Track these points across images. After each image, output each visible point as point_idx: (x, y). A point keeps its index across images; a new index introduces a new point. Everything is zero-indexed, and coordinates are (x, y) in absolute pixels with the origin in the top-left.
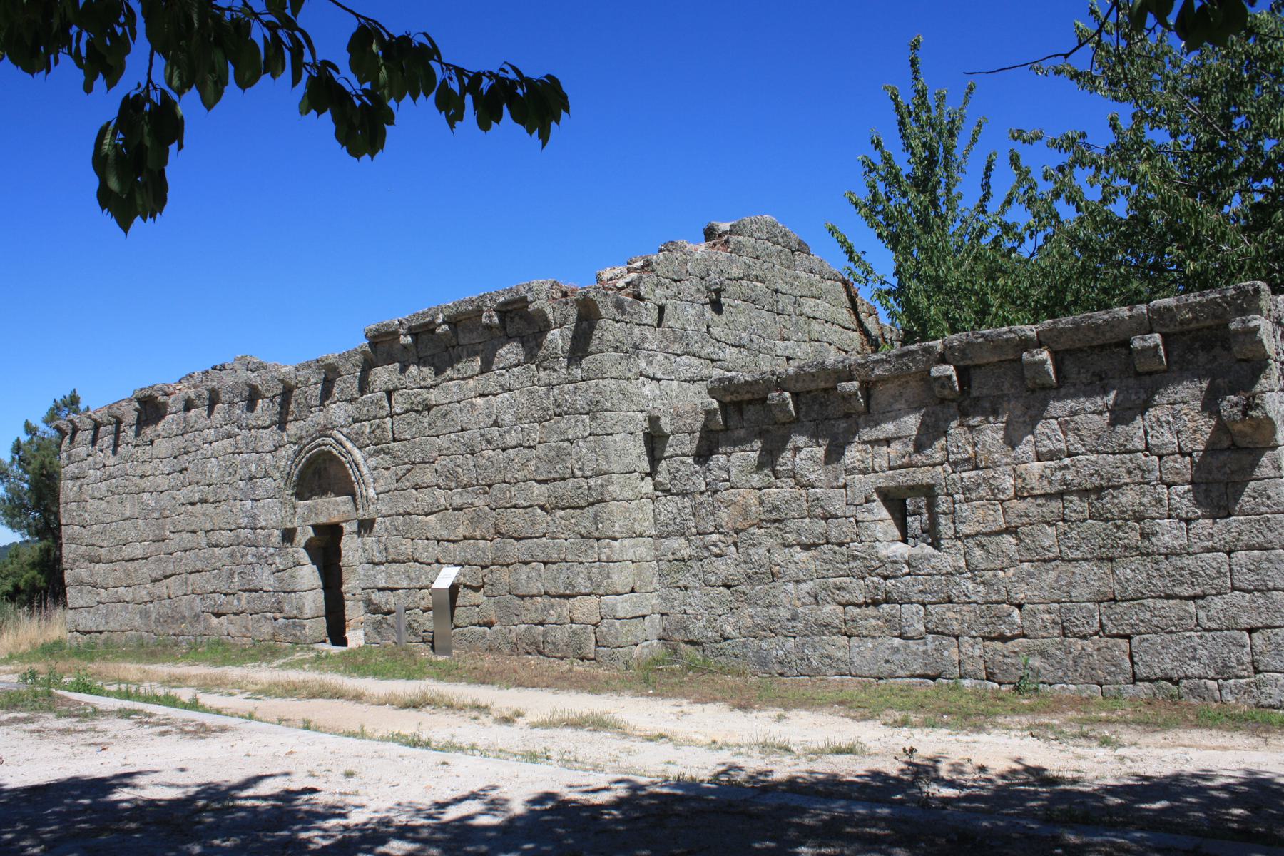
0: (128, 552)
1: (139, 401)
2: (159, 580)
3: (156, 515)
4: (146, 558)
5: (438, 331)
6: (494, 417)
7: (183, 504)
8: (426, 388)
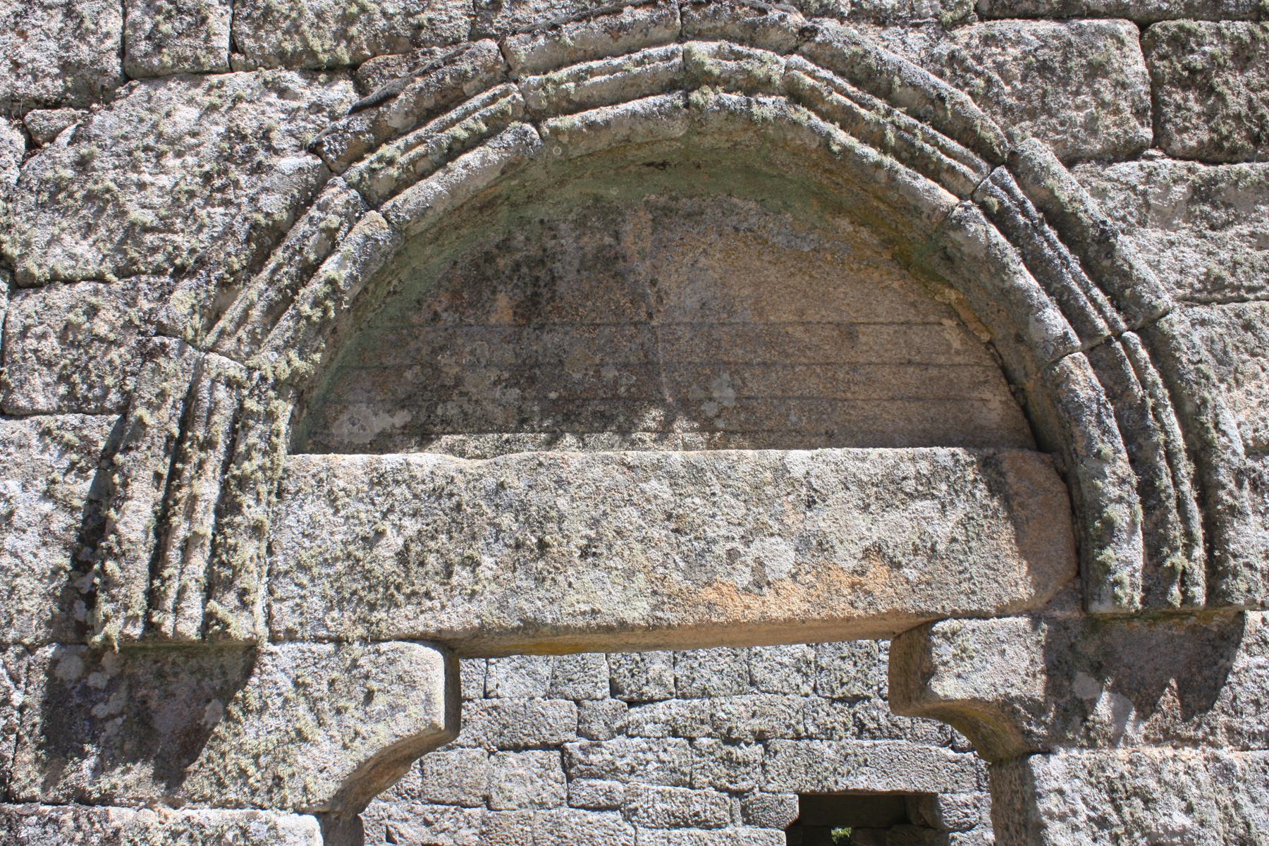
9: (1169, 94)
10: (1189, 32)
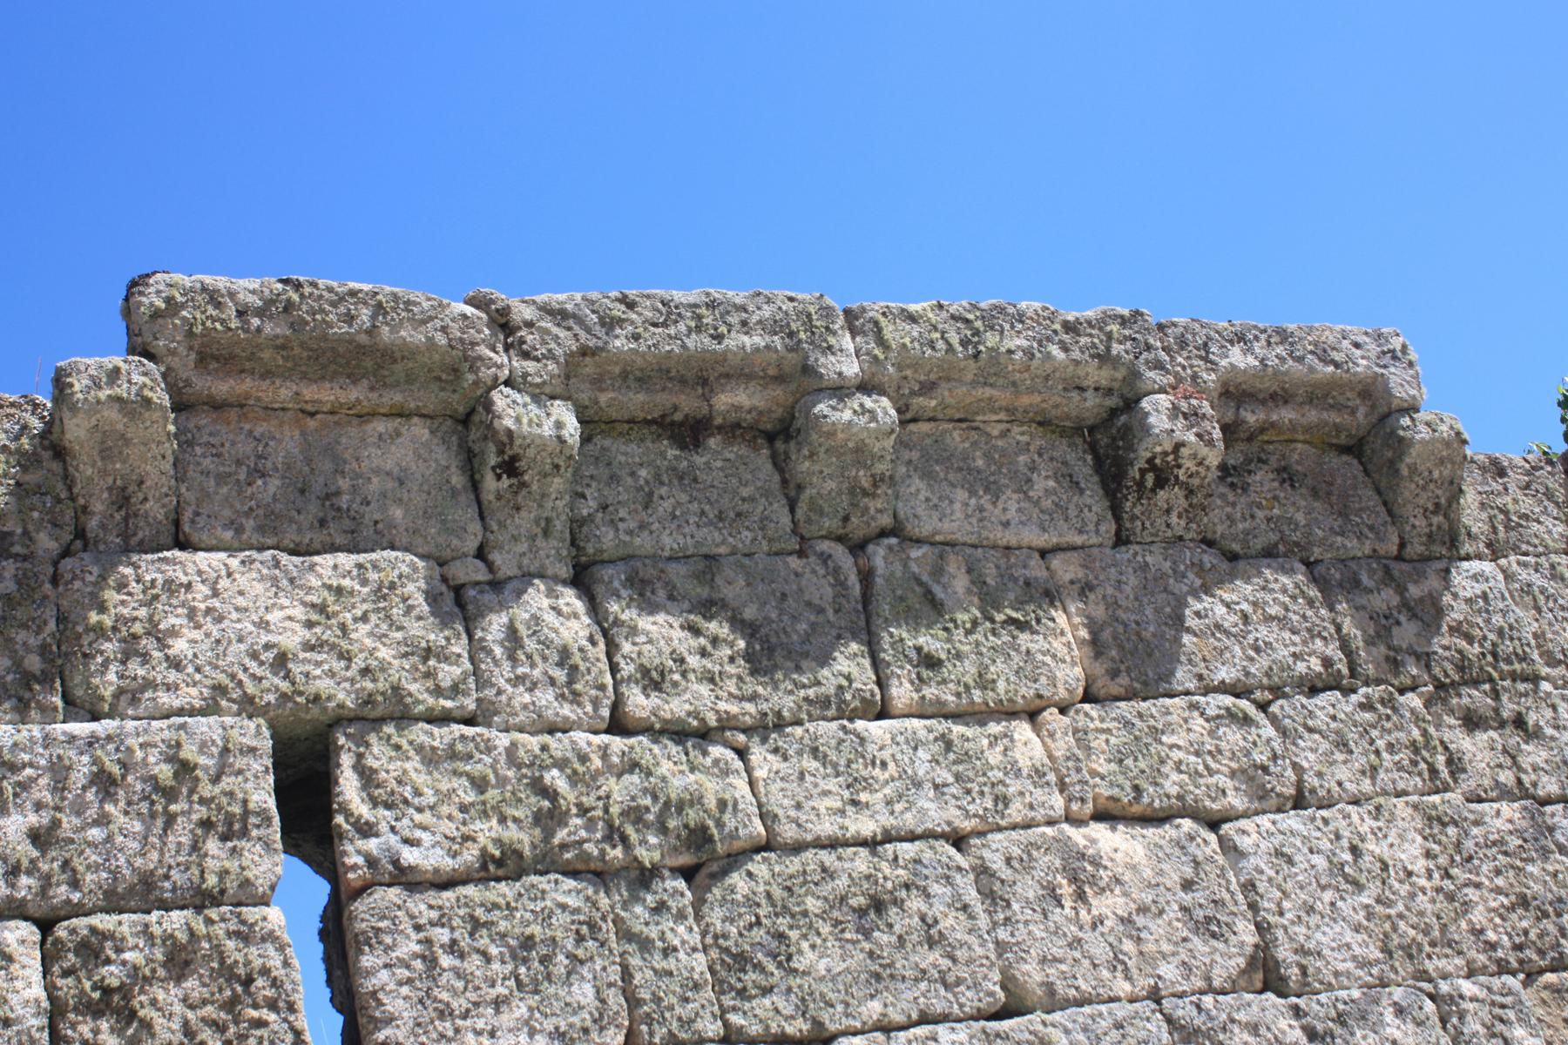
5: (839, 414)
6: (1247, 934)
8: (677, 732)
9: (73, 1026)
10: (104, 936)
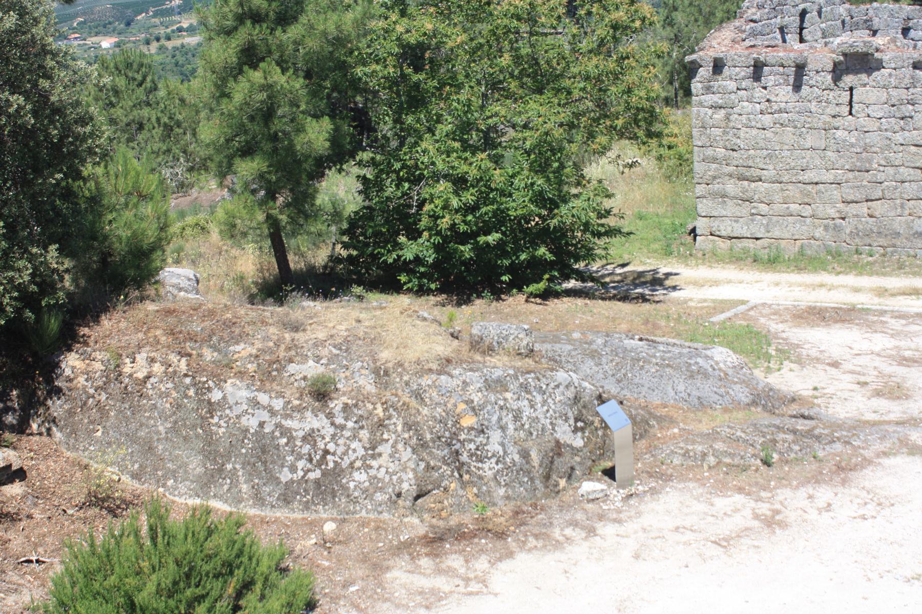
0: (809, 176)
1: (845, 55)
2: (857, 202)
3: (859, 150)
4: (839, 184)
7: (902, 145)
